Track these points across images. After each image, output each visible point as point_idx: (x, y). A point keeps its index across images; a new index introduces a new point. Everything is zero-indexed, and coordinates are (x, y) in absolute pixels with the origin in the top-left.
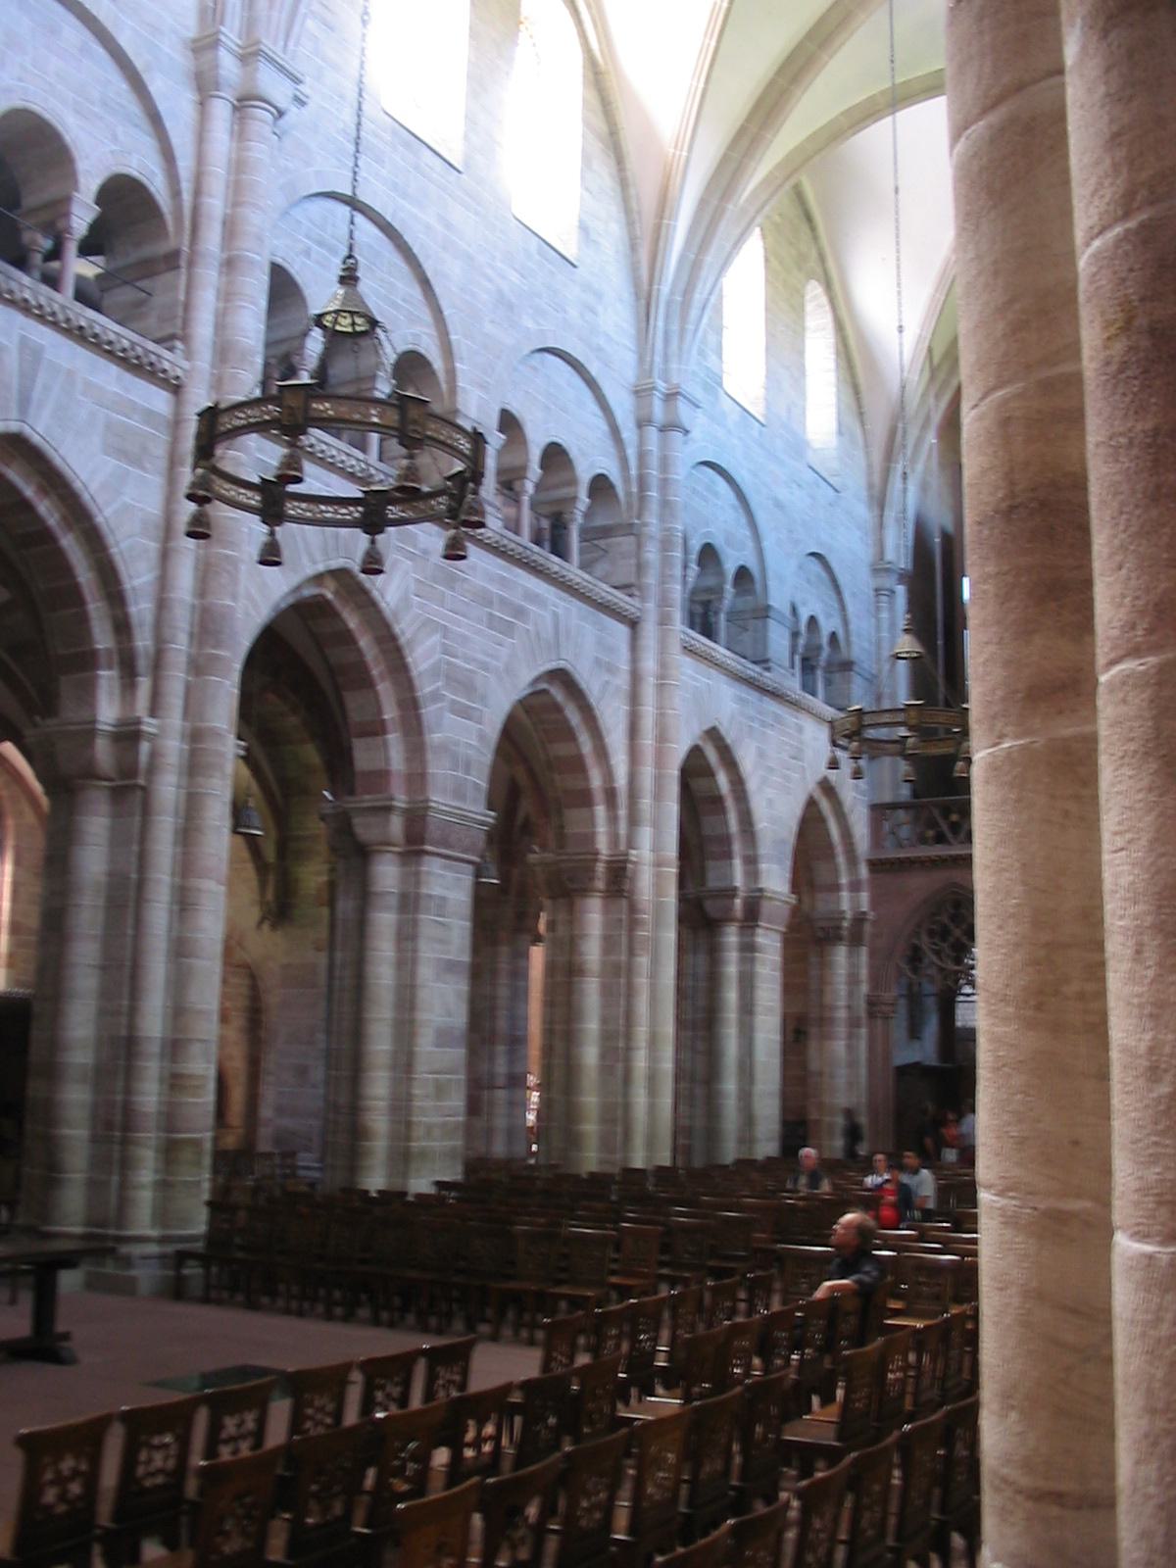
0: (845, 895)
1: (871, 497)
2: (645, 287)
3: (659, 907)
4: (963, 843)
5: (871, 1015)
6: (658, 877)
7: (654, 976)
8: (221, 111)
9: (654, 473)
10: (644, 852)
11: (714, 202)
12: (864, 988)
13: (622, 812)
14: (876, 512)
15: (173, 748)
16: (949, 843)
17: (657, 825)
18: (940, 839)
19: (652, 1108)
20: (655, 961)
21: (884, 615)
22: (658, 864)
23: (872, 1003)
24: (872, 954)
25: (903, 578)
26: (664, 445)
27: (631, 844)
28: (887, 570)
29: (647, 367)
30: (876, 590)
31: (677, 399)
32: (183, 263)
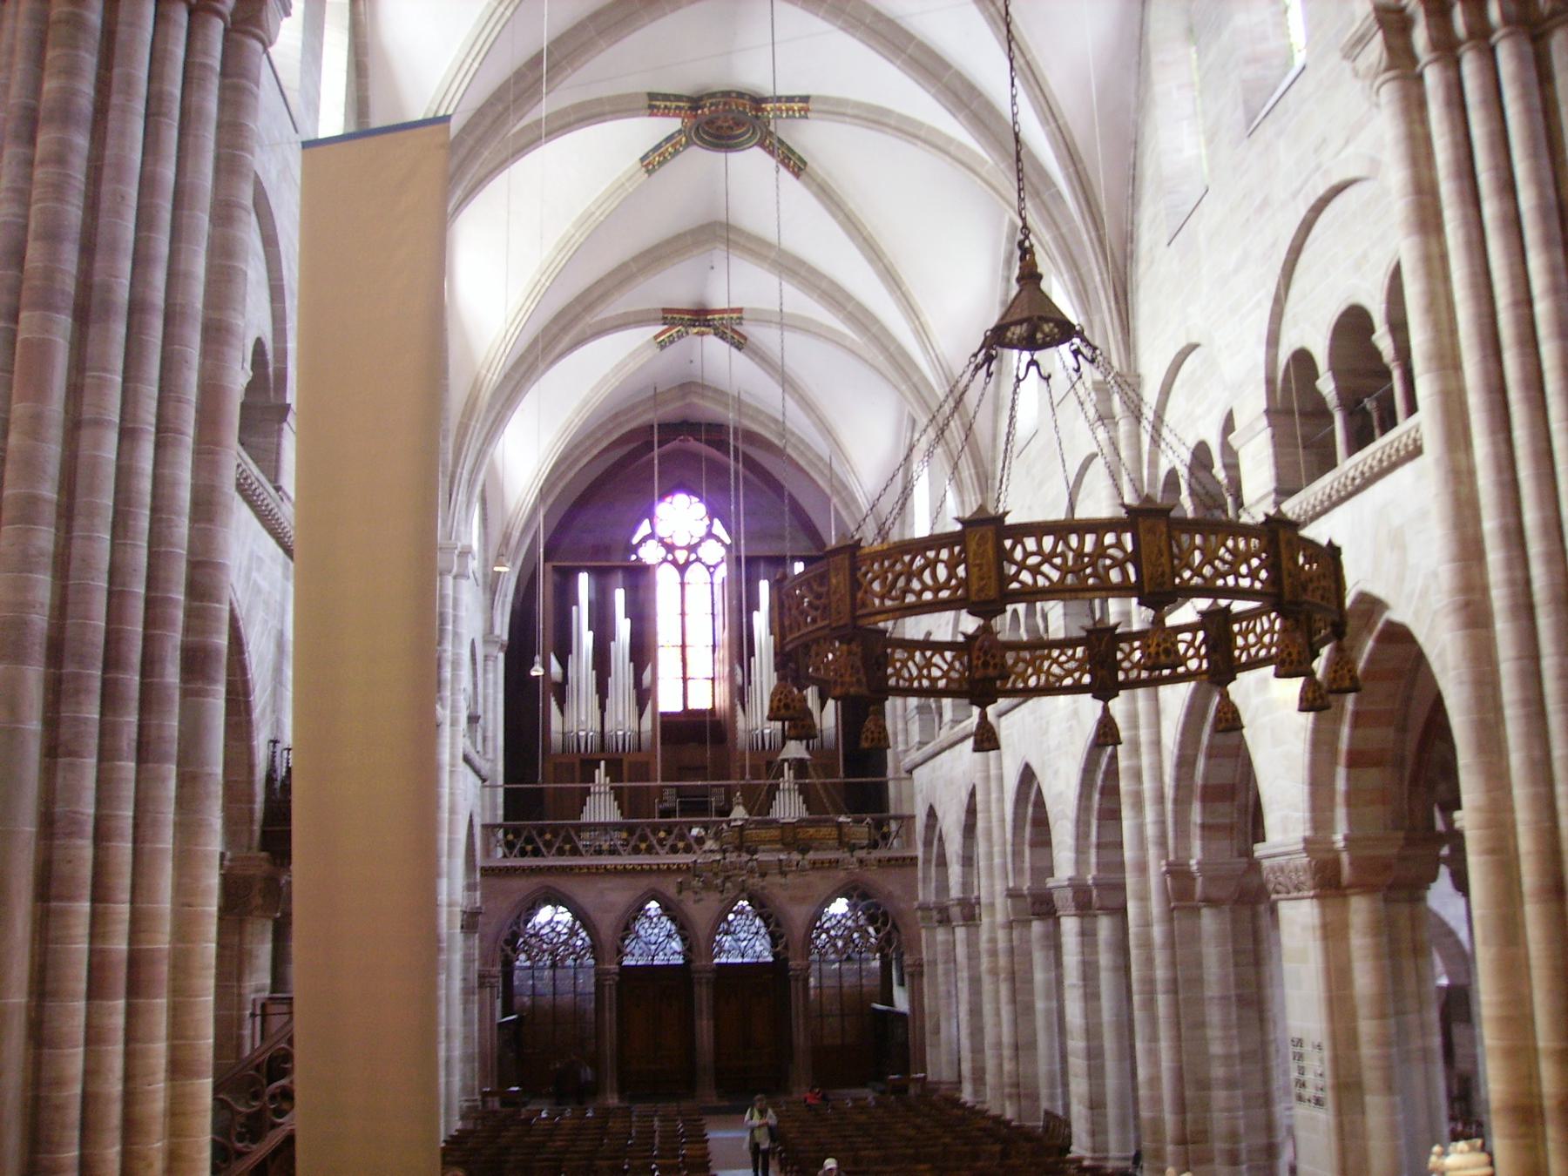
2: (450, 468)
3: (451, 936)
5: (481, 985)
6: (450, 914)
7: (448, 988)
9: (450, 611)
11: (498, 407)
12: (477, 964)
14: (488, 596)
16: (543, 856)
17: (450, 877)
18: (536, 853)
19: (448, 1083)
20: (449, 977)
21: (490, 676)
22: (450, 905)
23: (482, 976)
24: (481, 940)
26: (455, 587)
28: (496, 642)
29: (448, 530)
31: (467, 557)
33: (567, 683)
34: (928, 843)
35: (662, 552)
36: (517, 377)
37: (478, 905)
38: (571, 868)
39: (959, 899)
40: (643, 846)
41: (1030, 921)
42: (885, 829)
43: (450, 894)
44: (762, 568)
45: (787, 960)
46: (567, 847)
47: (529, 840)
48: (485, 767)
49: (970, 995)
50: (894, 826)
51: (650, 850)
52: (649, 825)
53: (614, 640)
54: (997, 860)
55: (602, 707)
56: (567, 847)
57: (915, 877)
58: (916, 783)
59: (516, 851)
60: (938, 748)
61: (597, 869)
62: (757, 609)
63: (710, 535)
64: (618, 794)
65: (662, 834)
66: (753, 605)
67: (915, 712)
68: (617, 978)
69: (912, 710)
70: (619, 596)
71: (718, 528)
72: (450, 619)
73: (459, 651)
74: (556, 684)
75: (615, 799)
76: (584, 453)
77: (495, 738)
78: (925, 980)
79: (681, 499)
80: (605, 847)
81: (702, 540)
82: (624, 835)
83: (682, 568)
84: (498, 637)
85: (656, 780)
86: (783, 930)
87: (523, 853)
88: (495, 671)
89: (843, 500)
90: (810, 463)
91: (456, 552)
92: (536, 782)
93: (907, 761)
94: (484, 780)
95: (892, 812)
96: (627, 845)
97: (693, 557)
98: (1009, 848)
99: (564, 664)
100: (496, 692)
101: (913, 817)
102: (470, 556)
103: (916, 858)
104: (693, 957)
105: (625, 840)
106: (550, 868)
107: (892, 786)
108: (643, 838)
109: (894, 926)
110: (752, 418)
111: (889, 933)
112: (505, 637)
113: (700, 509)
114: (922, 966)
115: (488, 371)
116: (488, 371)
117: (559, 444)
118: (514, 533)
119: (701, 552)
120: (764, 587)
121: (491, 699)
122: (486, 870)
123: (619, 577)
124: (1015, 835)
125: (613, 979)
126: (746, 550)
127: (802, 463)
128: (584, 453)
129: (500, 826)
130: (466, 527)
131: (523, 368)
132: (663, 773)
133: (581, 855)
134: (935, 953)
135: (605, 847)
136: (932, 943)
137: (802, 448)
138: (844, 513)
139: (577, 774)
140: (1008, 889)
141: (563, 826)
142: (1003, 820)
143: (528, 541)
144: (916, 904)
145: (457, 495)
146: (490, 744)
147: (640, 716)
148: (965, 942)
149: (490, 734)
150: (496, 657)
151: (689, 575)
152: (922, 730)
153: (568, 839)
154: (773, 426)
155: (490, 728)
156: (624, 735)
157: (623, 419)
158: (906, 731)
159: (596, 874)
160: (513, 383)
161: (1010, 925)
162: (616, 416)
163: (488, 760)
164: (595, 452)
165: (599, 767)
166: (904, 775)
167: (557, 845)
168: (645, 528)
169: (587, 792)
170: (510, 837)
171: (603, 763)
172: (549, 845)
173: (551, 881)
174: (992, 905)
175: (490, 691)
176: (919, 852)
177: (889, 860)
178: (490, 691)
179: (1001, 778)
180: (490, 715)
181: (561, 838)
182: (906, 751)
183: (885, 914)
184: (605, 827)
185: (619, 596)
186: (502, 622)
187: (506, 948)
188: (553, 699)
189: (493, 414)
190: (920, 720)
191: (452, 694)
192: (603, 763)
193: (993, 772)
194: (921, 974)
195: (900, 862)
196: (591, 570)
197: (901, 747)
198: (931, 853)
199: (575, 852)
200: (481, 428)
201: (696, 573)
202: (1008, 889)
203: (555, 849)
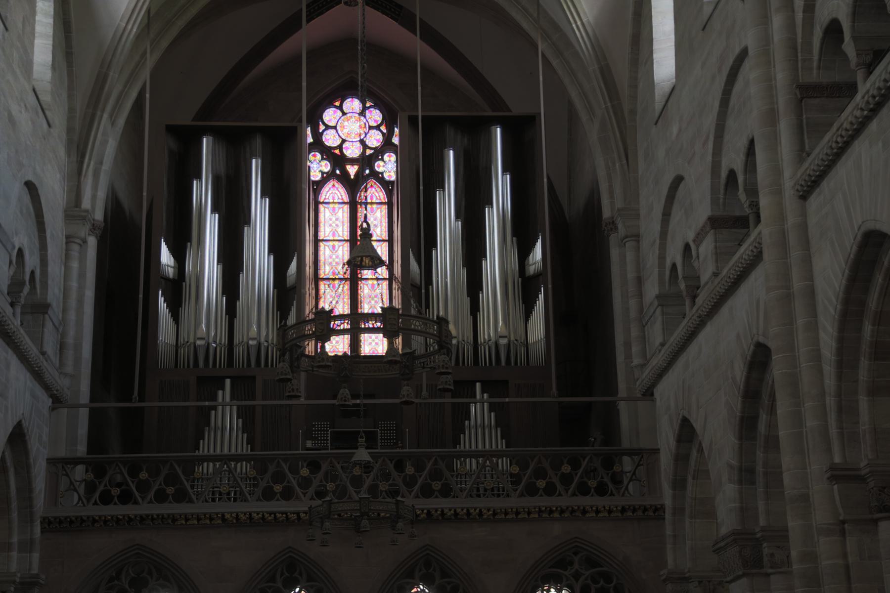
0: (15, 554)
1: (69, 142)
4: (151, 502)
16: (136, 503)
18: (126, 498)
25: (94, 227)
28: (84, 218)
30: (67, 237)
33: (184, 280)
34: (679, 484)
35: (326, 167)
37: (35, 571)
40: (278, 488)
41: (876, 521)
42: (616, 468)
44: (450, 132)
46: (170, 490)
48: (62, 383)
50: (627, 464)
51: (288, 494)
54: (811, 422)
56: (170, 490)
58: (658, 403)
61: (211, 519)
63: (387, 145)
66: (436, 181)
67: (656, 303)
69: (651, 304)
70: (255, 165)
74: (166, 279)
77: (78, 347)
79: (353, 105)
83: (353, 186)
84: (87, 211)
87: (106, 499)
92: (130, 401)
94: (57, 401)
95: (626, 444)
96: (255, 486)
98: (831, 402)
100: (81, 288)
101: (656, 451)
103: (663, 507)
105: (255, 479)
106: (142, 519)
107: (623, 408)
108: (279, 477)
112: (99, 216)
113: (375, 116)
119: (379, 167)
121: (74, 295)
122: (50, 523)
123: (258, 143)
124: (840, 377)
129: (76, 461)
133: (191, 501)
138: (555, 63)
140: (833, 467)
142: (817, 357)
143: (134, 95)
144: (664, 572)
146: (70, 354)
149: (70, 340)
150: (85, 241)
155: (71, 332)
156: (259, 344)
158: (643, 339)
161: (841, 528)
163: (66, 375)
165: (223, 388)
167: (156, 487)
169: (204, 416)
170: (91, 476)
171: (228, 382)
174: (805, 499)
175: (74, 284)
176: (667, 498)
177: (624, 510)
178: (74, 284)
179: (811, 293)
180: (72, 316)
182: (643, 366)
185: (255, 165)
186: (94, 197)
190: (663, 314)
192: (228, 382)
193: (797, 284)
195: (640, 513)
196: (218, 133)
197: (636, 361)
199: (182, 496)
202: (833, 467)
203: (151, 494)
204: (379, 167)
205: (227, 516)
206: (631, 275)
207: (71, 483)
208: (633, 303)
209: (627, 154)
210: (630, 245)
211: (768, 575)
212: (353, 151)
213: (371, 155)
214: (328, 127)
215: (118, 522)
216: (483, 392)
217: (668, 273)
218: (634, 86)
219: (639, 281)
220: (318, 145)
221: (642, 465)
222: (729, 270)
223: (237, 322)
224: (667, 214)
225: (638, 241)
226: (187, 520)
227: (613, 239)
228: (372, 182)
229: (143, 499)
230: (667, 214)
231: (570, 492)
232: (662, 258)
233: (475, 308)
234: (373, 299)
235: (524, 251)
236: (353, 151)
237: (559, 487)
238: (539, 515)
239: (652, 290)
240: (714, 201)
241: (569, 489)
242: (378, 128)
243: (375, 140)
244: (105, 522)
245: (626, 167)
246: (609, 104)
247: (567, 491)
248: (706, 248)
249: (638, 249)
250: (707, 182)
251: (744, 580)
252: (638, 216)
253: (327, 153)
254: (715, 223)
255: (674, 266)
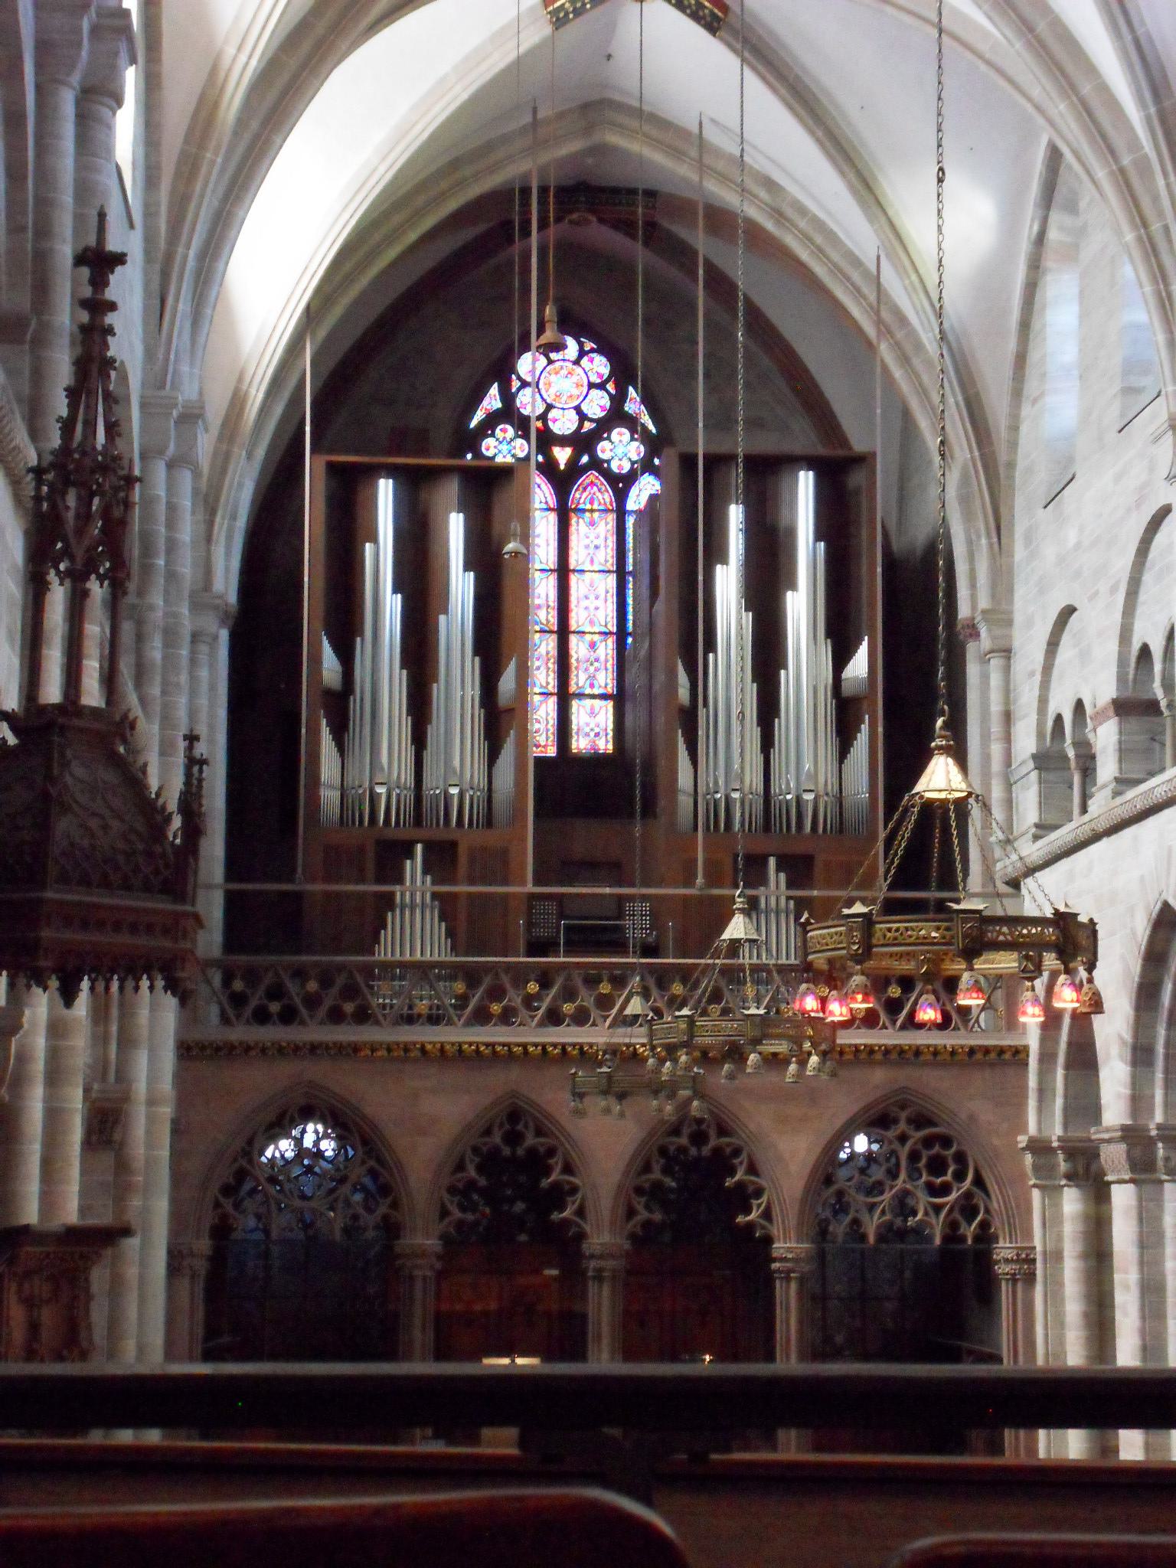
2: (162, 244)
4: (322, 1023)
6: (151, 1119)
7: (143, 1264)
8: (67, 102)
10: (141, 1088)
11: (255, 125)
13: (114, 1028)
15: (40, 1043)
16: (303, 1023)
18: (288, 1016)
21: (204, 673)
22: (152, 1102)
27: (123, 1076)
32: (28, 337)
36: (293, 63)
38: (356, 1048)
39: (1125, 1129)
43: (152, 1079)
45: (768, 1240)
46: (349, 1008)
47: (276, 992)
49: (1143, 1318)
52: (508, 967)
53: (446, 611)
55: (419, 740)
56: (349, 1008)
57: (1024, 1087)
59: (248, 1011)
60: (1085, 832)
62: (724, 561)
63: (616, 416)
64: (447, 907)
65: (533, 987)
67: (1031, 765)
68: (438, 1265)
69: (1023, 762)
70: (456, 526)
71: (634, 404)
72: (161, 544)
73: (174, 609)
74: (328, 693)
75: (441, 919)
76: (390, 240)
78: (1039, 1289)
80: (422, 1007)
81: (604, 426)
82: (460, 987)
83: (563, 481)
84: (220, 597)
85: (523, 882)
86: (763, 1182)
87: (262, 1017)
88: (212, 666)
89: (897, 346)
90: (836, 270)
91: (175, 413)
92: (291, 880)
93: (1006, 865)
97: (585, 459)
99: (346, 655)
100: (212, 705)
102: (200, 422)
104: (587, 1228)
106: (314, 1048)
109: (979, 1182)
110: (724, 178)
111: (968, 1195)
112: (232, 598)
113: (600, 366)
114: (1034, 1261)
115: (239, 49)
116: (239, 49)
117: (346, 216)
118: (253, 391)
119: (604, 450)
120: (735, 515)
122: (189, 1049)
125: (432, 1267)
126: (707, 442)
127: (819, 270)
128: (390, 240)
130: (192, 365)
131: (306, 46)
132: (536, 872)
134: (1060, 1238)
135: (422, 1007)
136: (1053, 1220)
137: (819, 240)
139: (370, 866)
141: (341, 968)
143: (278, 410)
144: (1022, 1140)
145: (177, 300)
147: (493, 755)
148: (1134, 1213)
150: (216, 638)
151: (579, 496)
152: (1045, 800)
153: (351, 991)
154: (763, 194)
157: (467, 171)
158: (1009, 803)
159: (405, 1060)
160: (286, 77)
162: (455, 164)
164: (413, 236)
165: (410, 855)
166: (1003, 888)
168: (492, 400)
169: (387, 902)
170: (238, 985)
171: (419, 847)
172: (312, 1002)
173: (316, 1071)
176: (1033, 1041)
177: (972, 1051)
181: (334, 991)
183: (961, 1158)
184: (422, 971)
186: (227, 569)
187: (222, 1199)
188: (324, 722)
189: (247, 137)
191: (164, 693)
192: (419, 847)
194: (1030, 1278)
198: (1057, 1042)
199: (363, 1016)
200: (223, 170)
201: (593, 494)
203: (322, 1012)
204: (604, 450)
205: (429, 1047)
206: (996, 707)
207: (214, 992)
208: (996, 749)
209: (999, 527)
210: (996, 663)
211: (1161, 1182)
212: (564, 423)
213: (591, 431)
214: (525, 384)
215: (283, 1051)
216: (778, 870)
217: (1050, 723)
218: (1014, 428)
219: (1008, 717)
220: (508, 413)
221: (1000, 987)
222: (1136, 796)
223: (427, 756)
224: (1053, 645)
225: (1009, 658)
226: (373, 1050)
227: (972, 650)
228: (593, 476)
229: (311, 1017)
230: (1053, 645)
231: (899, 1023)
232: (1043, 701)
233: (767, 743)
234: (592, 664)
235: (841, 658)
236: (564, 423)
237: (883, 1017)
238: (855, 1056)
239: (1026, 743)
240: (1121, 679)
241: (897, 1020)
242: (601, 386)
243: (597, 404)
244: (264, 1050)
245: (996, 546)
246: (976, 454)
247: (894, 1022)
248: (1106, 737)
249: (1007, 670)
250: (1113, 647)
251: (1132, 1186)
252: (1009, 623)
253: (522, 425)
254: (1122, 707)
255: (1059, 719)
